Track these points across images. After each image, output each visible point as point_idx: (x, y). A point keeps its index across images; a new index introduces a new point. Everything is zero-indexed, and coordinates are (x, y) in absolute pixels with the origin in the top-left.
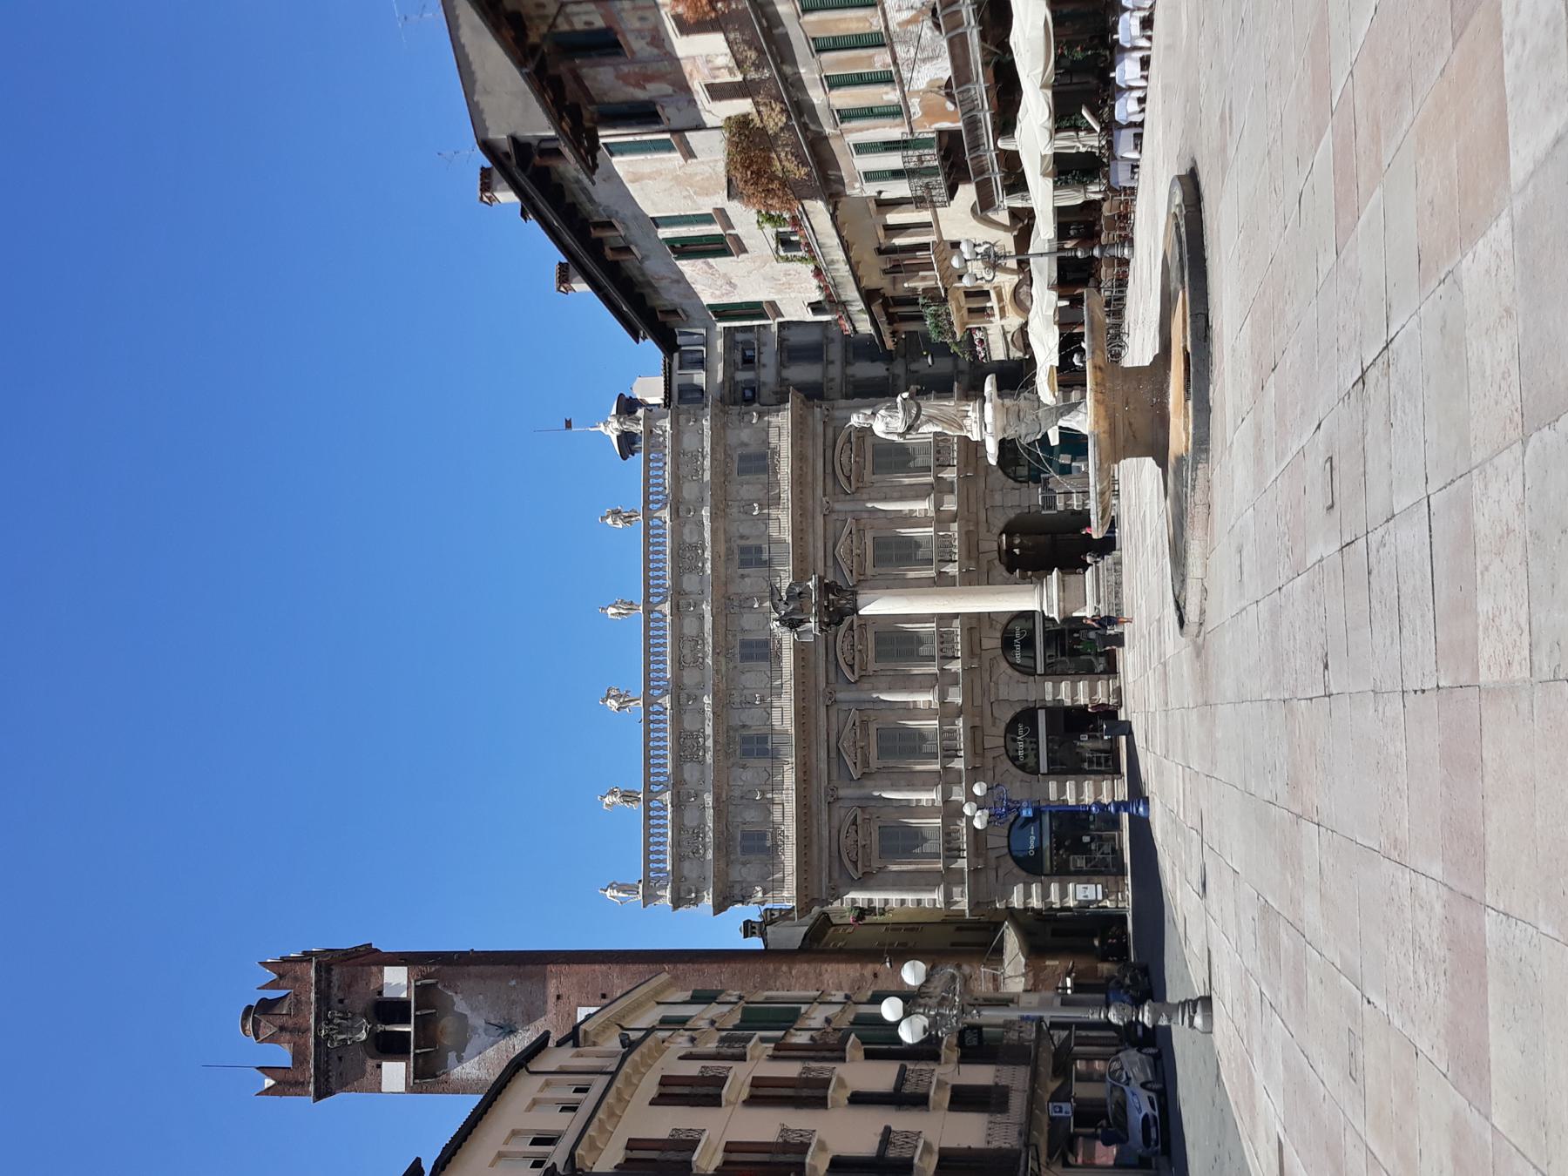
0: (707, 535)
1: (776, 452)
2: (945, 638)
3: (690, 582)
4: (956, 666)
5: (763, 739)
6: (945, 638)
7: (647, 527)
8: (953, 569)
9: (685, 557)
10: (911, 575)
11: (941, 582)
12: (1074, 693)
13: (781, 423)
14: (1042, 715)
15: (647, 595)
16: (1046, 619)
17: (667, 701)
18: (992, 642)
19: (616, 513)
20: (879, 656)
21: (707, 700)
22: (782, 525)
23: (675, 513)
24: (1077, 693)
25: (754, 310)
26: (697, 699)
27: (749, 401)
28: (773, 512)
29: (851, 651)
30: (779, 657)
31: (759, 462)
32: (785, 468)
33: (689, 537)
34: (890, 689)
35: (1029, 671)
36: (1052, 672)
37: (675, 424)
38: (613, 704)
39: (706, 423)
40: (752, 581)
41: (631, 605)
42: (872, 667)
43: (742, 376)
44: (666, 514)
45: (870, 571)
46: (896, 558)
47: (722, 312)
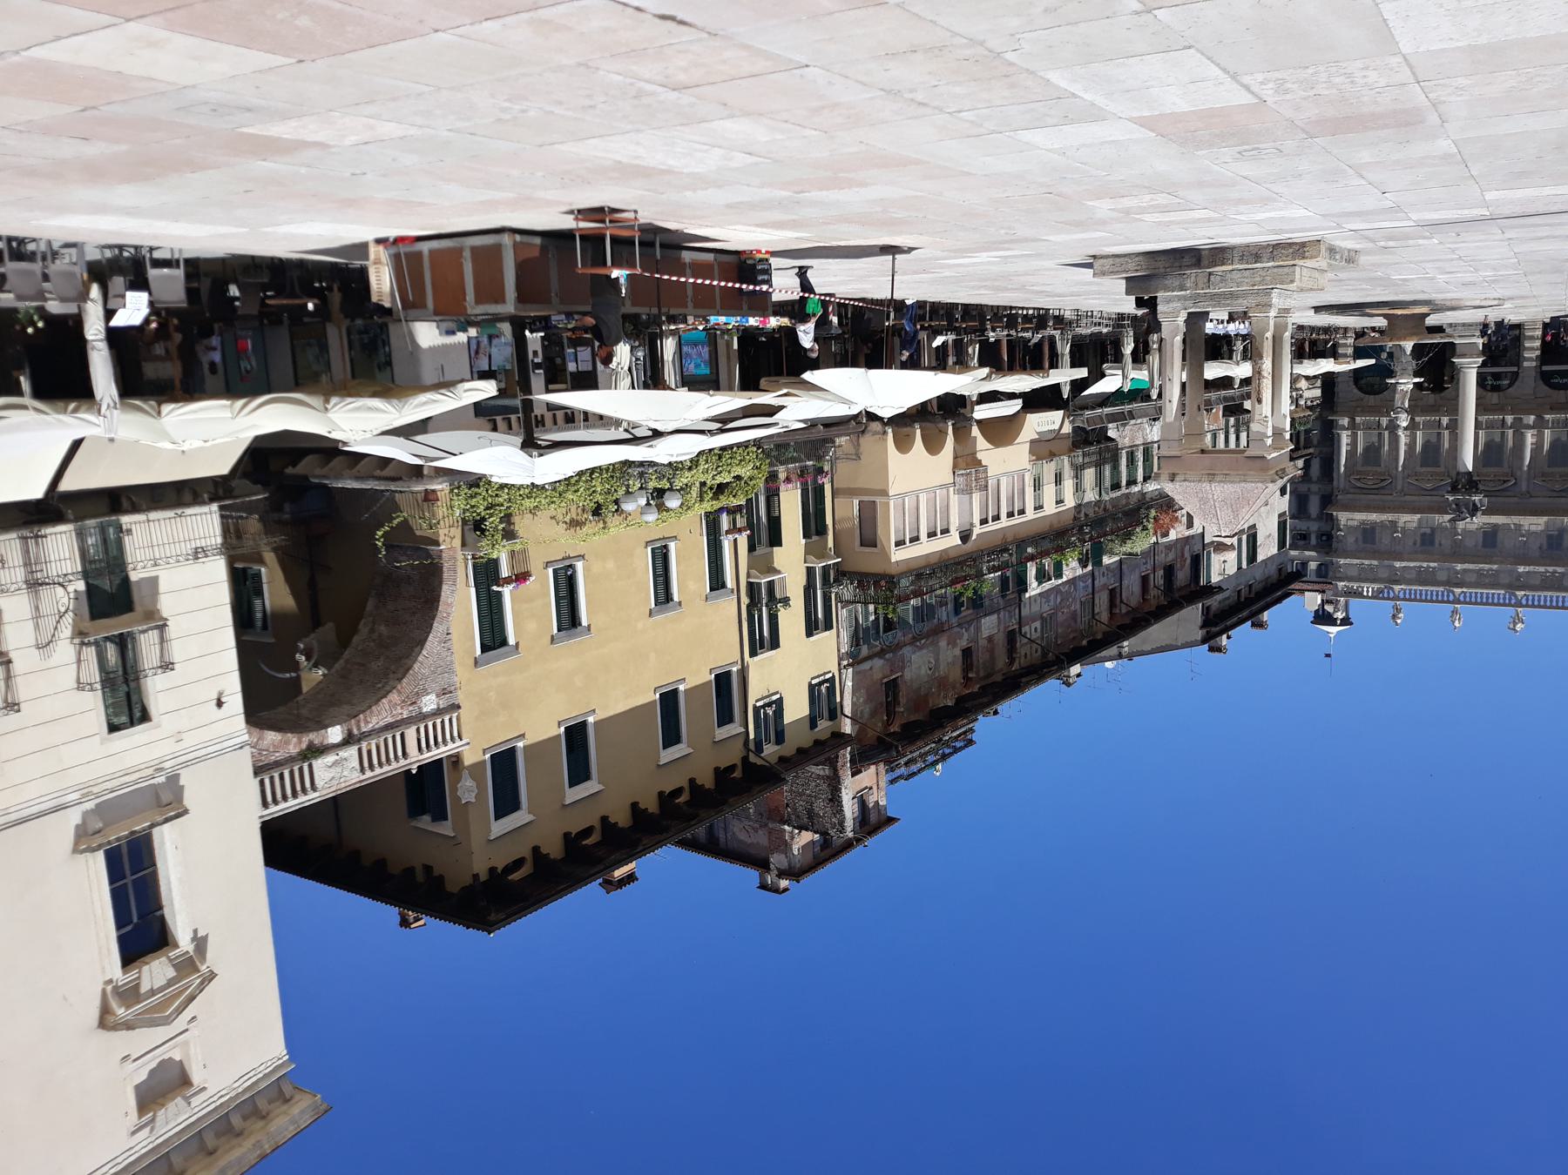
0: (1412, 564)
1: (1363, 523)
2: (1490, 426)
3: (1442, 576)
4: (1509, 419)
5: (1550, 537)
6: (1490, 426)
7: (1405, 599)
8: (1445, 420)
9: (1424, 578)
10: (1446, 445)
11: (1454, 427)
12: (1532, 349)
13: (1344, 518)
14: (1545, 368)
15: (1448, 602)
16: (1484, 364)
17: (1520, 594)
18: (1494, 398)
19: (1394, 617)
20: (1499, 463)
21: (1521, 569)
22: (1409, 520)
23: (1397, 582)
24: (1532, 348)
25: (1282, 526)
26: (1520, 575)
27: (1330, 537)
28: (1401, 524)
29: (1495, 479)
30: (1496, 525)
31: (1368, 533)
32: (1374, 517)
33: (1413, 575)
34: (1522, 458)
35: (1515, 377)
36: (1517, 361)
37: (1341, 580)
38: (1519, 626)
39: (1342, 561)
40: (1443, 541)
41: (1455, 612)
42: (1506, 469)
43: (1313, 541)
44: (1397, 588)
45: (1442, 469)
46: (1433, 455)
47: (1282, 544)
